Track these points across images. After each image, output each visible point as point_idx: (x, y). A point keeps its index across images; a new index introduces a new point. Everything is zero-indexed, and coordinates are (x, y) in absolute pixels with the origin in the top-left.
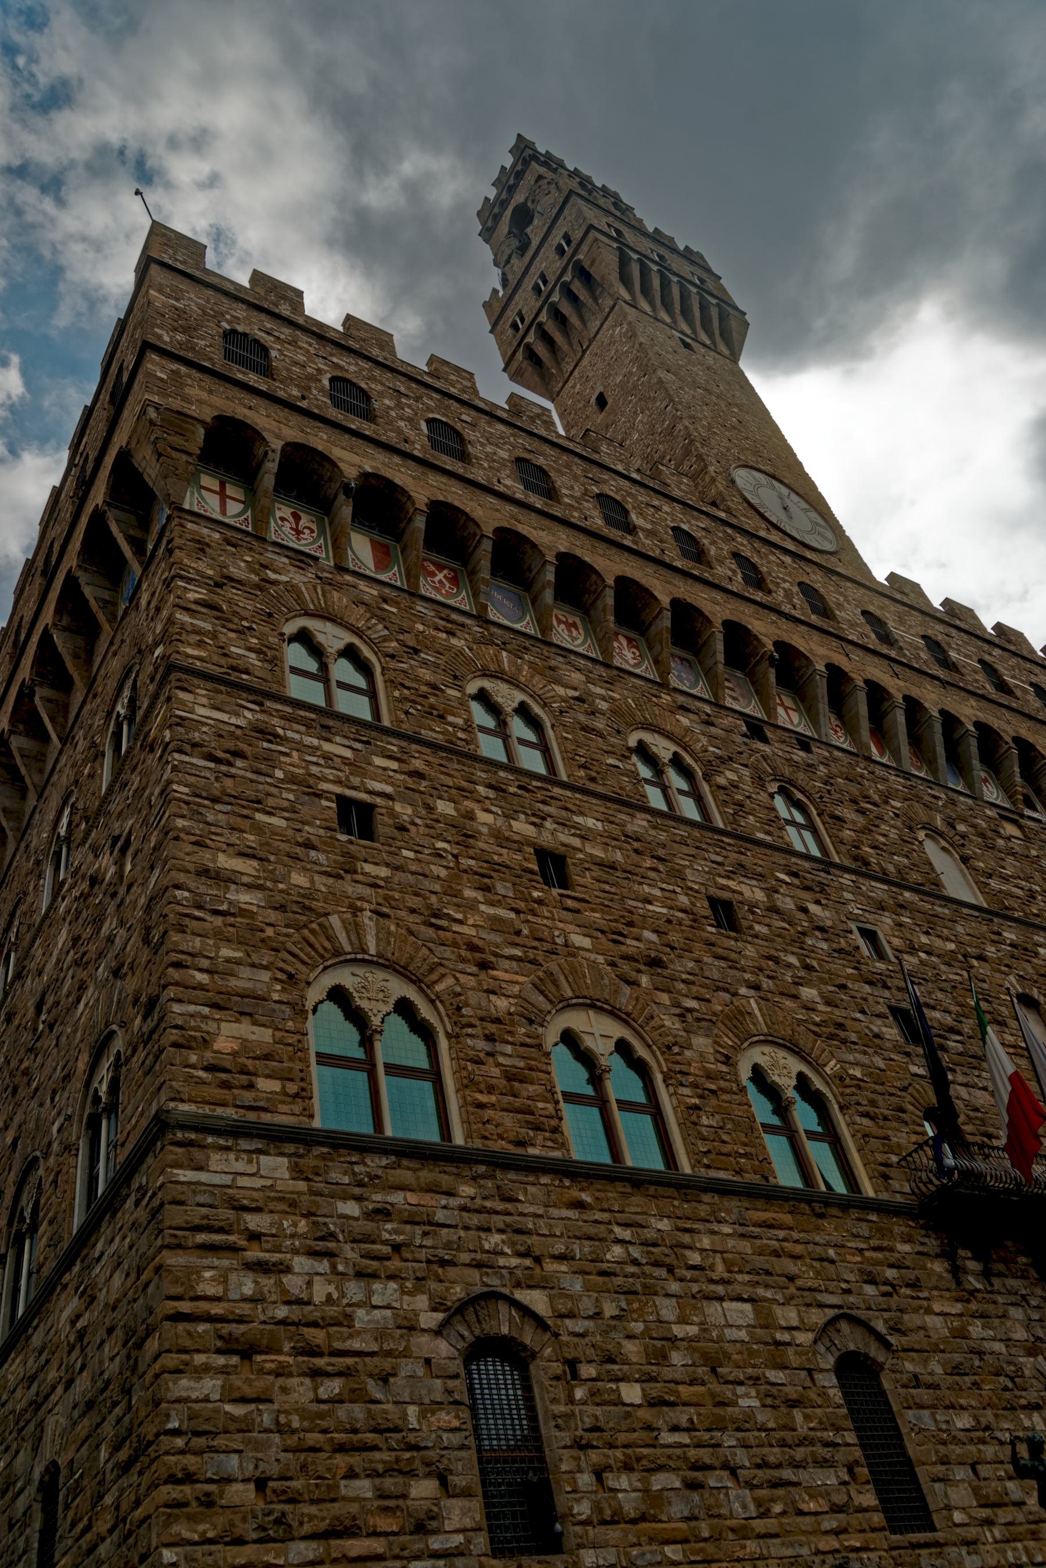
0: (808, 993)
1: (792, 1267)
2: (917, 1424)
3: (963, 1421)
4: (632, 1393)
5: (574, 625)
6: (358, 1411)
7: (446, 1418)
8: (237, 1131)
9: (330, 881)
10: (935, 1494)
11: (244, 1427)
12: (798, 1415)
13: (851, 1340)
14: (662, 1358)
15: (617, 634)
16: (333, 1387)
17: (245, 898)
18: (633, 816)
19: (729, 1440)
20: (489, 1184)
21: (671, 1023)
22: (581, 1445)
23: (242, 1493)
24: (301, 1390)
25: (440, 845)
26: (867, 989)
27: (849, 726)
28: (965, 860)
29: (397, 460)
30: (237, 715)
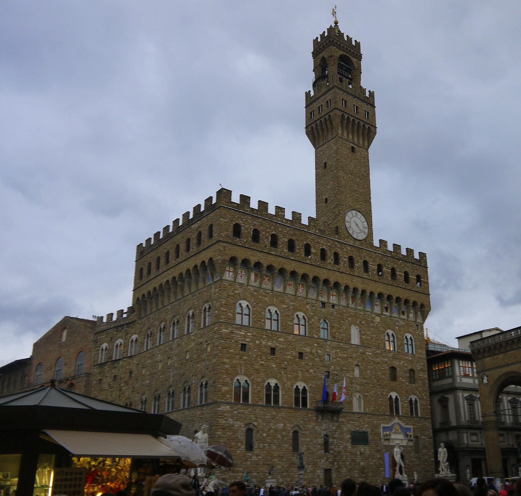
1: (291, 419)
2: (301, 439)
3: (308, 440)
4: (265, 435)
5: (291, 285)
6: (234, 436)
7: (243, 437)
8: (224, 403)
9: (238, 361)
10: (300, 448)
11: (223, 437)
13: (296, 429)
14: (269, 430)
16: (232, 433)
21: (285, 380)
22: (257, 440)
24: (228, 433)
26: (323, 368)
27: (347, 299)
28: (360, 331)
29: (262, 254)
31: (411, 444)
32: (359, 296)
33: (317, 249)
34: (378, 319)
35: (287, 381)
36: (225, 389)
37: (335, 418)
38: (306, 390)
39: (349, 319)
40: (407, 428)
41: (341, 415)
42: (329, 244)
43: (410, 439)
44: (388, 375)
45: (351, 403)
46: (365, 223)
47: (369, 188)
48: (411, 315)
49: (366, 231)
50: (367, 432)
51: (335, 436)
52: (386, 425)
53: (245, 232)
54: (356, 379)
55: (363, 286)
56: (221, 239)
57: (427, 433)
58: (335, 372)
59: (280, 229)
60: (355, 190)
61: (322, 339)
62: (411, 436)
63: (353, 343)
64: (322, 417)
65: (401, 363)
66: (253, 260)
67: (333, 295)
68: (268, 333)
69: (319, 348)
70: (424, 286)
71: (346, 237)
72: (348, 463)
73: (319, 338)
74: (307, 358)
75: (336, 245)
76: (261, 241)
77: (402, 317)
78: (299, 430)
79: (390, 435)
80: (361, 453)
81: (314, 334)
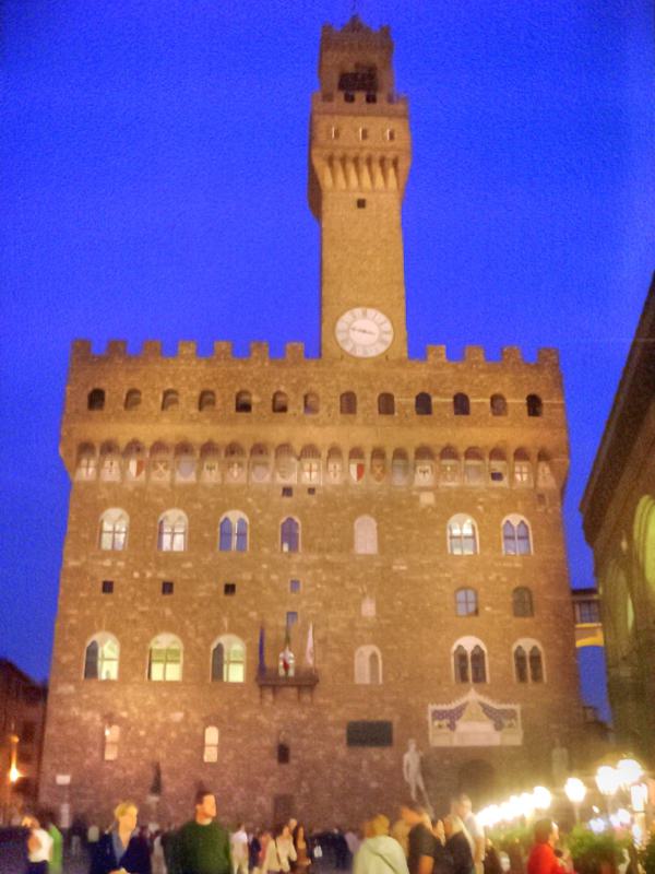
0: (253, 614)
4: (142, 733)
5: (214, 468)
17: (73, 621)
28: (378, 528)
32: (367, 462)
35: (197, 635)
37: (306, 698)
42: (294, 381)
45: (348, 669)
46: (388, 326)
49: (389, 338)
51: (305, 731)
58: (310, 612)
65: (491, 578)
67: (311, 471)
72: (335, 784)
77: (496, 484)
79: (452, 727)
80: (372, 764)
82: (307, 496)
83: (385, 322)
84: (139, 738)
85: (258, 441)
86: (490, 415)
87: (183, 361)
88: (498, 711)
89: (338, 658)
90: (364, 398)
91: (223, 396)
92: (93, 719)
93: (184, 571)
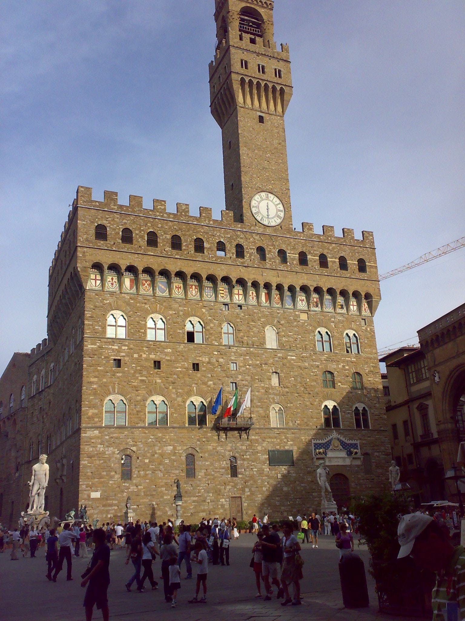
2: (198, 463)
4: (147, 461)
6: (105, 464)
7: (117, 465)
10: (197, 473)
12: (175, 463)
14: (154, 455)
15: (192, 286)
16: (102, 461)
18: (180, 345)
19: (161, 467)
20: (130, 431)
21: (174, 396)
23: (90, 474)
24: (98, 462)
25: (133, 365)
30: (95, 345)
31: (358, 463)
33: (213, 243)
34: (304, 317)
36: (91, 412)
37: (244, 436)
38: (205, 406)
39: (262, 320)
40: (351, 444)
41: (251, 432)
42: (229, 236)
43: (355, 456)
44: (320, 381)
46: (281, 207)
47: (285, 163)
48: (353, 308)
49: (282, 214)
50: (292, 451)
52: (320, 442)
53: (111, 234)
54: (273, 388)
55: (279, 279)
56: (79, 244)
57: (383, 448)
58: (244, 382)
59: (160, 225)
60: (264, 168)
61: (225, 346)
62: (356, 453)
63: (268, 346)
64: (226, 435)
66: (123, 264)
67: (238, 294)
68: (151, 345)
69: (222, 356)
70: (370, 272)
71: (253, 225)
73: (220, 345)
74: (204, 369)
75: (237, 236)
76: (134, 241)
77: (339, 311)
78: (194, 453)
81: (213, 340)
82: (238, 310)
83: (279, 204)
84: (145, 464)
85: (210, 272)
86: (339, 269)
87: (158, 214)
88: (348, 444)
89: (261, 411)
90: (270, 251)
91: (186, 241)
92: (114, 453)
93: (167, 354)
